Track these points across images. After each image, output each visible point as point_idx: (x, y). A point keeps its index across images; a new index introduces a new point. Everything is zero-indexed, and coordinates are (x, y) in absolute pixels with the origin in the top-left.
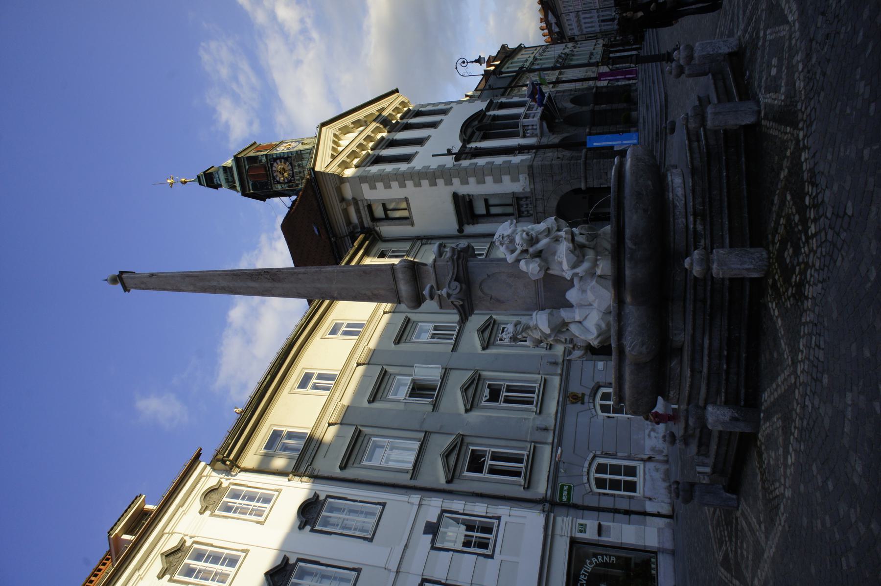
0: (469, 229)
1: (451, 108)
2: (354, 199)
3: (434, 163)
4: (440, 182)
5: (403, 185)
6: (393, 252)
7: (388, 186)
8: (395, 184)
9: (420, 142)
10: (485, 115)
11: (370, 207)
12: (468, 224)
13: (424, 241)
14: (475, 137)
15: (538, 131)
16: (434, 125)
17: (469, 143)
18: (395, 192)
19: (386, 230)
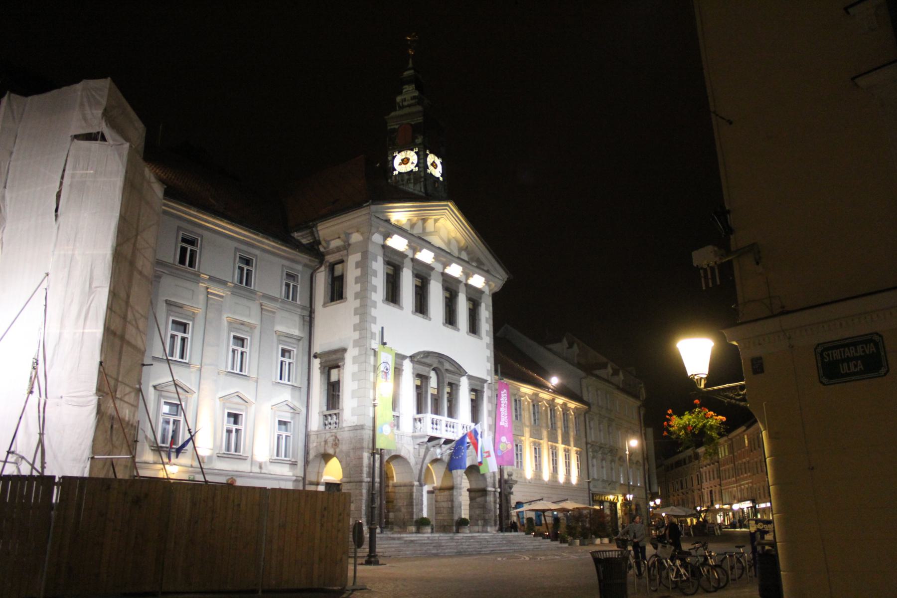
0: (316, 363)
1: (481, 338)
2: (349, 245)
3: (376, 329)
4: (356, 335)
5: (357, 296)
6: (295, 287)
7: (357, 280)
8: (358, 288)
9: (421, 307)
10: (462, 376)
11: (342, 262)
12: (321, 363)
13: (308, 319)
14: (417, 366)
15: (417, 434)
16: (450, 319)
17: (412, 361)
18: (351, 287)
19: (322, 279)
